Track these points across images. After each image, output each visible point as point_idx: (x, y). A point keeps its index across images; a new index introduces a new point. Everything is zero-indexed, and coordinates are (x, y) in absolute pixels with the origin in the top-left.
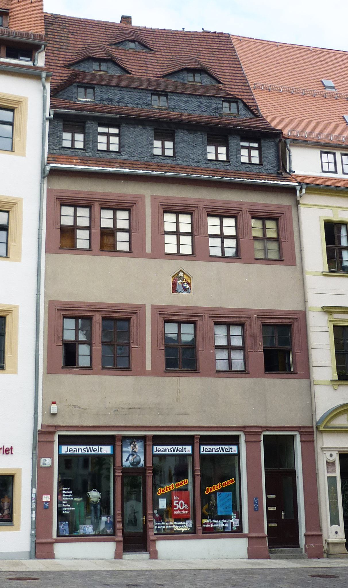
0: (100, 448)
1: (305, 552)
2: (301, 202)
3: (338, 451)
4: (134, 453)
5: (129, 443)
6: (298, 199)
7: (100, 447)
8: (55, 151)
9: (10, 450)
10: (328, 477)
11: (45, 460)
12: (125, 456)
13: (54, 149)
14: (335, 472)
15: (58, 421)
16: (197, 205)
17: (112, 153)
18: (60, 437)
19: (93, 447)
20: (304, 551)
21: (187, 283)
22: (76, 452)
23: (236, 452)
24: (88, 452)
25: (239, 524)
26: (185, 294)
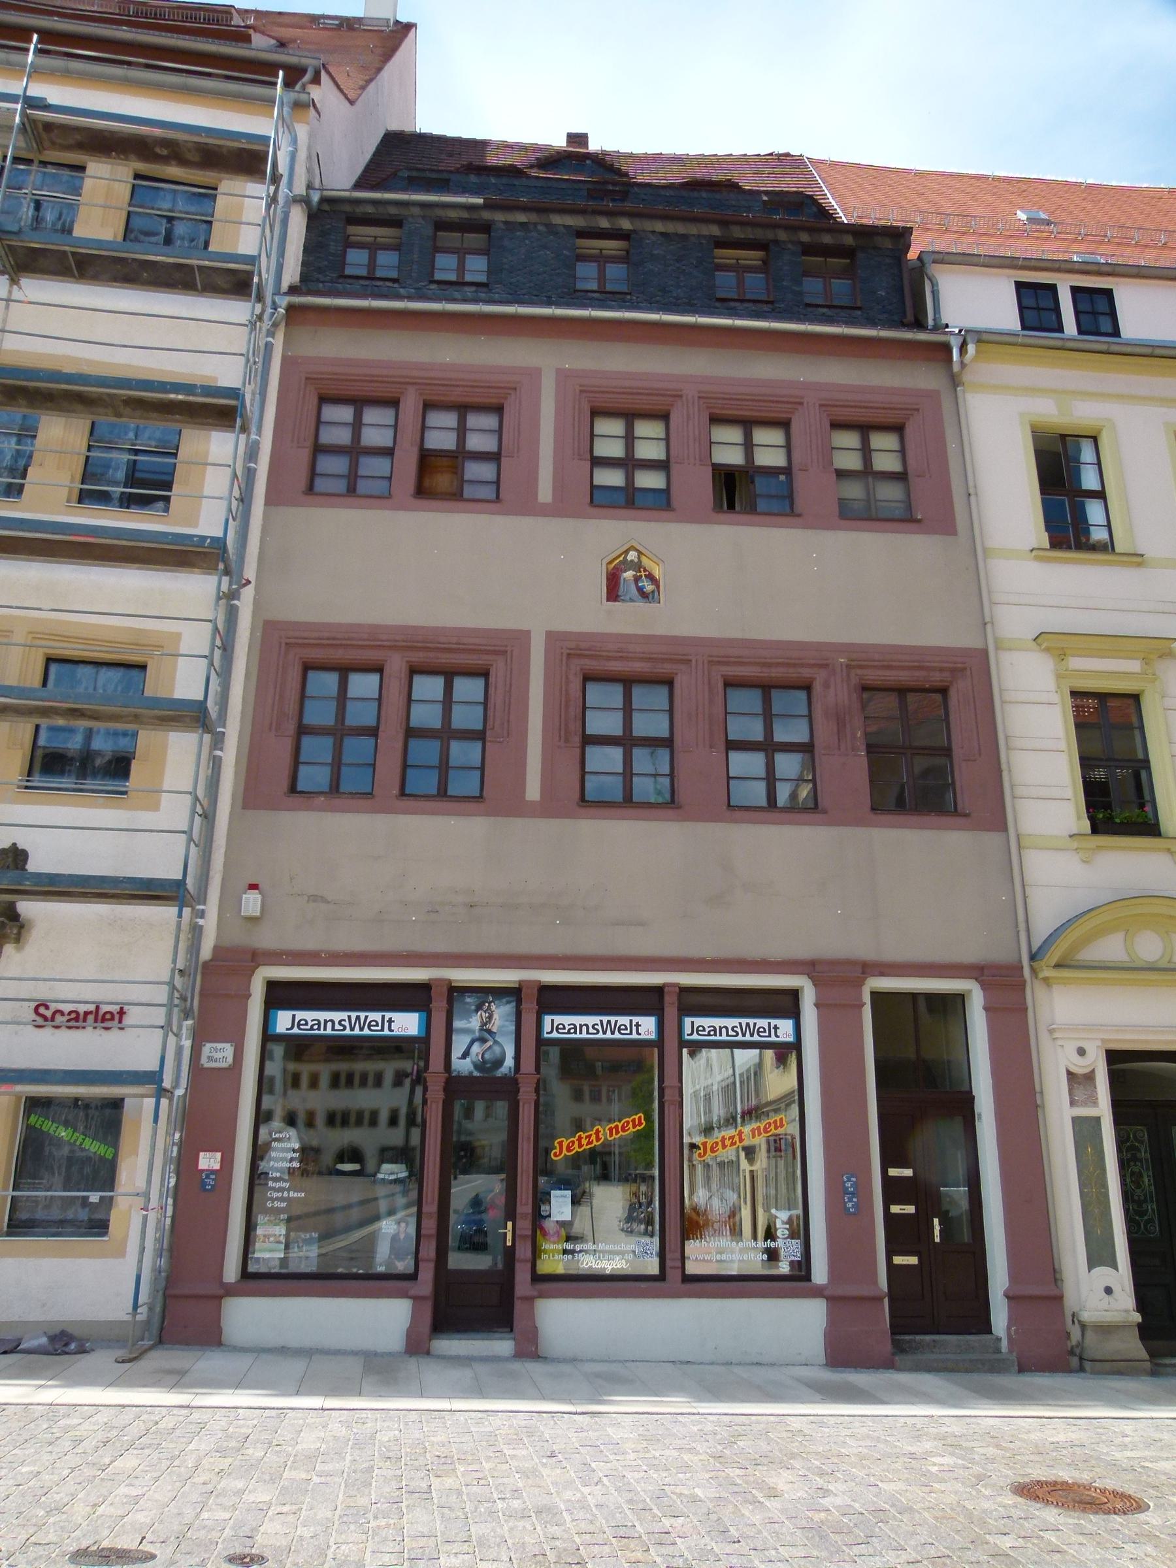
0: (386, 1019)
1: (1011, 1351)
2: (967, 377)
3: (1103, 1041)
4: (487, 1036)
5: (473, 1007)
6: (956, 368)
7: (388, 1015)
8: (321, 285)
10: (1076, 1120)
11: (216, 1050)
12: (459, 1044)
13: (318, 281)
14: (1095, 1103)
15: (266, 940)
16: (681, 390)
17: (467, 289)
19: (366, 1017)
20: (1004, 1345)
21: (651, 577)
22: (319, 1029)
23: (791, 1039)
24: (352, 1029)
25: (799, 1255)
26: (641, 605)
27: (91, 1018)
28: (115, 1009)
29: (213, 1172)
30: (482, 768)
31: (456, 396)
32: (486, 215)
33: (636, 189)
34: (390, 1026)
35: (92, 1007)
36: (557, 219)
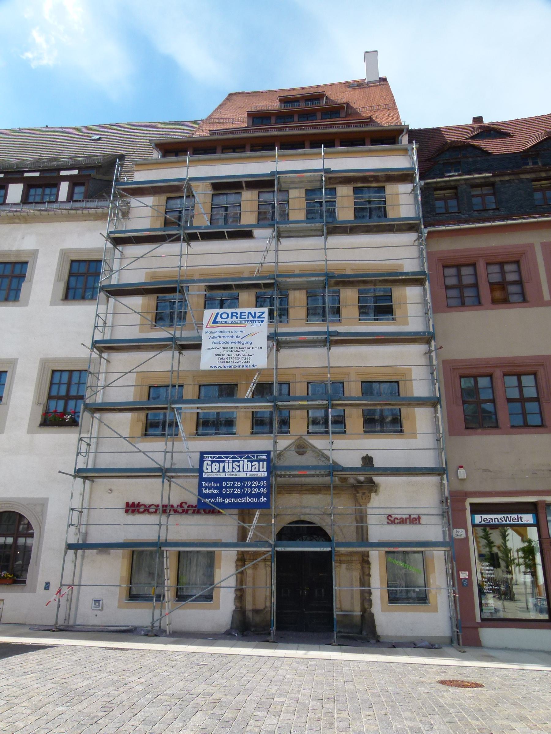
0: (519, 517)
8: (429, 219)
9: (417, 520)
11: (458, 532)
13: (428, 217)
15: (469, 487)
18: (471, 504)
27: (408, 520)
28: (416, 517)
29: (466, 579)
30: (541, 413)
31: (499, 259)
32: (492, 179)
33: (542, 152)
34: (521, 520)
35: (408, 516)
36: (523, 176)
